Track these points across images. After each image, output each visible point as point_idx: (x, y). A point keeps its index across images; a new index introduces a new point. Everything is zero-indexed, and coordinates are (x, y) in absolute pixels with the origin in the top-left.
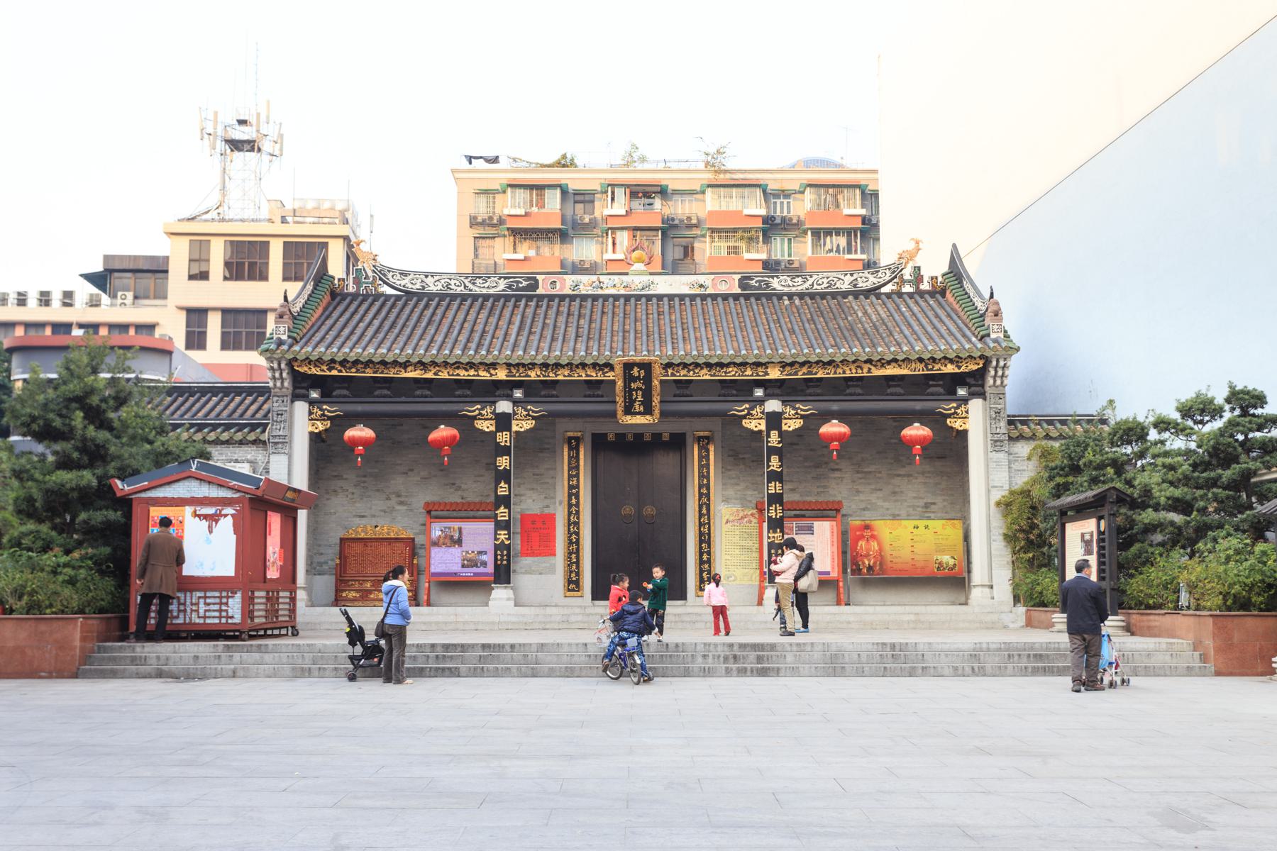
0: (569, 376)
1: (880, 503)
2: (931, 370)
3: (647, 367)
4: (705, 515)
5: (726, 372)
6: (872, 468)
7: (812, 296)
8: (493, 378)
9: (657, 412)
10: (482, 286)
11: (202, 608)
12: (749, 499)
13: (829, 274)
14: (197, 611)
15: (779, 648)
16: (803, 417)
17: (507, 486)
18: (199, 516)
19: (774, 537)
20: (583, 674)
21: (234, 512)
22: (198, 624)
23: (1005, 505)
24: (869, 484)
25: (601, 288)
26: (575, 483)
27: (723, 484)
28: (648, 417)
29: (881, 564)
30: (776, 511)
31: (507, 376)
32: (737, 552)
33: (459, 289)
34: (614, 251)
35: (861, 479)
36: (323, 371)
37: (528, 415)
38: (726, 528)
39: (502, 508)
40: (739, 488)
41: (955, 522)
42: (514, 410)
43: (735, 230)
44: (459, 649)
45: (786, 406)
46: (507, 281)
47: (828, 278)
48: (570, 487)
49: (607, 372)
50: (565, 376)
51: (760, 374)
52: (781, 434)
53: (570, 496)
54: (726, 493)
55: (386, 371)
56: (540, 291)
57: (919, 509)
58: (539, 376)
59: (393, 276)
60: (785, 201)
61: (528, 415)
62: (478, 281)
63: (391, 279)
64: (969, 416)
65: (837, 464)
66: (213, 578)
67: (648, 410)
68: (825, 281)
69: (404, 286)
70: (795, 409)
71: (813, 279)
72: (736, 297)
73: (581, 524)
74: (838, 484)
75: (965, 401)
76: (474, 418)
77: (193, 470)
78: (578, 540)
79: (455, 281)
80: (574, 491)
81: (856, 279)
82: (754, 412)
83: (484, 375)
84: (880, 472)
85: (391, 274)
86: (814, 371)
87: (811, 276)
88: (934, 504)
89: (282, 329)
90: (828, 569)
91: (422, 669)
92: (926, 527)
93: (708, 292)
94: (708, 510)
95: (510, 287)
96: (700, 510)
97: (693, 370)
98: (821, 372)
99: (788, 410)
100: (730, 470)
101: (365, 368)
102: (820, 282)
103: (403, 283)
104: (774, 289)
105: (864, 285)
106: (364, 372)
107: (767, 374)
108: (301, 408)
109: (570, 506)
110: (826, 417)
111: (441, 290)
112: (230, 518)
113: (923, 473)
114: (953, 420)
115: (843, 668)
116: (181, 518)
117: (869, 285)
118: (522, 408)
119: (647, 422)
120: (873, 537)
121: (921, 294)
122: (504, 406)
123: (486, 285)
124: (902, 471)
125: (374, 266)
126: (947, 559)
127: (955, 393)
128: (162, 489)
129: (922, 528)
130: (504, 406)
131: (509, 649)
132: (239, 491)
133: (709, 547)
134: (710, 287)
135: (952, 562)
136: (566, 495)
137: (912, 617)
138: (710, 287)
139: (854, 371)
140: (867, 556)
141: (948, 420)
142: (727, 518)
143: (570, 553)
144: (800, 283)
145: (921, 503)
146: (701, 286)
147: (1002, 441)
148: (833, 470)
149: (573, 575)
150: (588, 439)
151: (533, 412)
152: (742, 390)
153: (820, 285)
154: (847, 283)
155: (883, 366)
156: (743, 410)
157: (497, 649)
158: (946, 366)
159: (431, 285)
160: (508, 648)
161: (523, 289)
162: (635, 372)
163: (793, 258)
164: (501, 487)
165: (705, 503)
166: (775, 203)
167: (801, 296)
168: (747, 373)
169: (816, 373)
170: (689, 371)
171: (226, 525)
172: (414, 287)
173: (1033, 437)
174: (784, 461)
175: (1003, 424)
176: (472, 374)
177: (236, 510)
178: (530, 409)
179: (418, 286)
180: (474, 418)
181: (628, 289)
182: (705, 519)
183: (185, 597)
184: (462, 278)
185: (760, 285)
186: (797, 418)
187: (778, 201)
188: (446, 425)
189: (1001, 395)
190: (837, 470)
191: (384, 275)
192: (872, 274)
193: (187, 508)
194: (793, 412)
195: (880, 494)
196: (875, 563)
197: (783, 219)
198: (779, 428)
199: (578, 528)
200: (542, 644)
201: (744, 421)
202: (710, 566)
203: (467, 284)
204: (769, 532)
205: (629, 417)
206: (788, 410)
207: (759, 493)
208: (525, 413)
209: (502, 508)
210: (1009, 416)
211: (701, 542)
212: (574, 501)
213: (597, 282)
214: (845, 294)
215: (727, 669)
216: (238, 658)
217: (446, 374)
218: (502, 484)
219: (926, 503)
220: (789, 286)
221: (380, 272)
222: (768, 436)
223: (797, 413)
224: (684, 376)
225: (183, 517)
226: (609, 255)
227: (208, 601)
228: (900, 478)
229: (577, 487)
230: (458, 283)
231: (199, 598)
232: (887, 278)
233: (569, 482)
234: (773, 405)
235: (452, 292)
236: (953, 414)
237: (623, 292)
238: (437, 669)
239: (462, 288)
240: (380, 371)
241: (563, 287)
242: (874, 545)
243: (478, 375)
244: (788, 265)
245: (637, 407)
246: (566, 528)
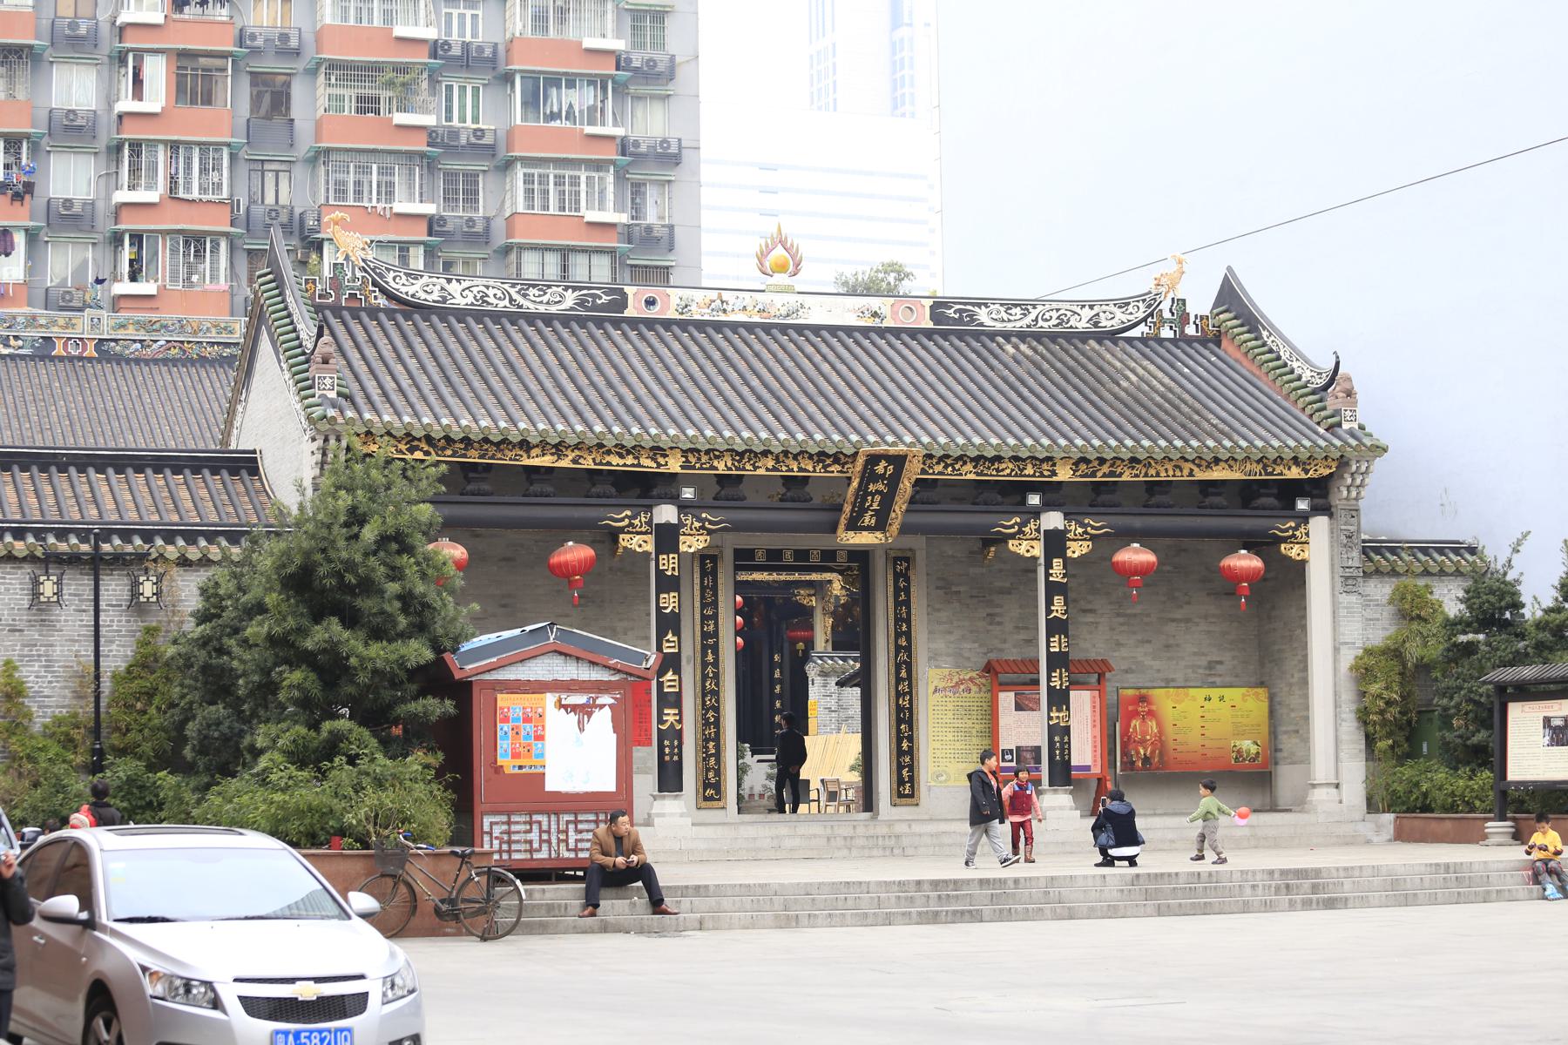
0: (774, 469)
1: (1148, 662)
2: (1271, 474)
3: (899, 461)
4: (904, 680)
5: (997, 470)
6: (1138, 609)
7: (1038, 337)
8: (662, 470)
9: (894, 528)
10: (538, 300)
11: (572, 837)
12: (967, 655)
13: (1060, 305)
14: (566, 841)
15: (1324, 875)
16: (1093, 538)
17: (675, 639)
18: (565, 707)
19: (1058, 717)
20: (1129, 914)
21: (612, 701)
22: (568, 859)
23: (1364, 672)
24: (1134, 633)
25: (725, 311)
26: (711, 628)
27: (930, 632)
28: (879, 534)
29: (1161, 754)
30: (1061, 679)
31: (682, 467)
32: (950, 736)
33: (502, 304)
35: (1122, 624)
36: (401, 452)
37: (703, 527)
38: (935, 699)
39: (671, 673)
40: (952, 638)
41: (1260, 690)
42: (679, 519)
43: (376, 67)
44: (951, 886)
45: (1070, 521)
46: (577, 293)
47: (1058, 310)
48: (705, 636)
49: (829, 465)
50: (767, 470)
51: (1046, 473)
52: (1067, 562)
53: (704, 649)
54: (933, 646)
55: (499, 456)
56: (630, 312)
57: (1201, 671)
58: (730, 469)
59: (394, 279)
60: (469, 13)
61: (703, 527)
62: (532, 291)
63: (392, 284)
64: (1311, 540)
65: (1090, 602)
66: (587, 794)
67: (881, 526)
68: (1055, 314)
69: (413, 296)
70: (1083, 525)
71: (1037, 311)
72: (928, 334)
73: (721, 694)
74: (1091, 633)
75: (1304, 518)
76: (622, 530)
77: (552, 640)
78: (717, 719)
79: (495, 291)
80: (711, 641)
81: (1098, 314)
82: (1027, 530)
83: (648, 464)
84: (1148, 615)
85: (392, 274)
86: (1119, 470)
87: (1034, 307)
88: (1221, 663)
89: (328, 381)
90: (1088, 762)
91: (936, 913)
92: (1221, 699)
93: (885, 324)
94: (909, 672)
95: (581, 303)
96: (898, 672)
97: (952, 465)
98: (1127, 473)
99: (1073, 528)
100: (939, 610)
101: (466, 449)
102: (1047, 316)
103: (411, 290)
104: (981, 324)
105: (1109, 324)
106: (464, 456)
107: (1054, 473)
109: (705, 664)
110: (1125, 536)
111: (472, 304)
112: (607, 711)
113: (1206, 617)
114: (1288, 546)
115: (1415, 895)
116: (540, 710)
117: (1115, 324)
118: (693, 516)
119: (877, 541)
120: (1151, 714)
121: (1189, 341)
122: (666, 513)
123: (545, 299)
124: (1178, 614)
125: (364, 260)
126: (1248, 746)
127: (1293, 506)
128: (513, 668)
129: (1215, 699)
130: (666, 513)
131: (1012, 886)
132: (619, 671)
133: (911, 729)
134: (889, 316)
135: (1254, 749)
136: (699, 647)
137: (1246, 832)
138: (889, 316)
139: (1171, 473)
140: (1143, 742)
141: (1283, 546)
142: (935, 683)
143: (706, 740)
144: (1018, 317)
145: (1203, 661)
146: (875, 315)
147: (1354, 578)
148: (1085, 611)
149: (711, 775)
150: (728, 556)
151: (711, 523)
152: (1015, 492)
153: (1046, 320)
154: (1085, 320)
155: (1208, 466)
156: (1012, 527)
157: (997, 886)
158: (1289, 469)
159: (457, 295)
160: (1011, 884)
161: (603, 308)
162: (880, 469)
163: (481, 126)
164: (668, 641)
165: (905, 662)
166: (449, 15)
167: (1022, 336)
168: (1026, 472)
169: (1120, 475)
170: (946, 467)
171: (602, 720)
172: (429, 298)
173: (1394, 573)
174: (1071, 606)
175: (1355, 554)
176: (629, 463)
177: (615, 699)
178: (706, 519)
179: (435, 296)
180: (622, 530)
181: (765, 314)
182: (903, 687)
183: (549, 821)
184: (506, 286)
185: (961, 317)
186: (1085, 540)
187: (455, 12)
188: (576, 542)
189: (1354, 512)
190: (1091, 611)
191: (381, 276)
192: (1120, 307)
193: (548, 695)
194: (1080, 530)
195: (1148, 648)
196: (1153, 752)
197: (466, 46)
198: (1062, 554)
199: (718, 701)
200: (1052, 878)
201: (1011, 542)
202: (912, 759)
203: (515, 296)
204: (1050, 710)
205: (851, 534)
206: (1073, 528)
207: (980, 646)
208: (697, 525)
209: (671, 673)
210: (1364, 541)
211: (899, 721)
212: (710, 658)
213: (719, 302)
214: (1084, 337)
215: (1290, 900)
216: (688, 905)
217: (590, 459)
218: (670, 636)
219: (1210, 662)
220: (1003, 321)
221: (373, 270)
222: (1049, 565)
223: (1086, 532)
224: (940, 473)
225: (544, 708)
226: (126, 104)
227: (580, 826)
228: (1174, 624)
229: (716, 634)
230: (499, 294)
231: (568, 822)
232: (1141, 315)
233: (702, 628)
234: (1053, 520)
235: (489, 308)
236: (1290, 537)
237: (756, 319)
238: (955, 912)
239: (506, 302)
240: (490, 454)
241: (666, 307)
242: (1152, 725)
243: (639, 465)
244: (473, 140)
245: (867, 519)
246: (699, 701)
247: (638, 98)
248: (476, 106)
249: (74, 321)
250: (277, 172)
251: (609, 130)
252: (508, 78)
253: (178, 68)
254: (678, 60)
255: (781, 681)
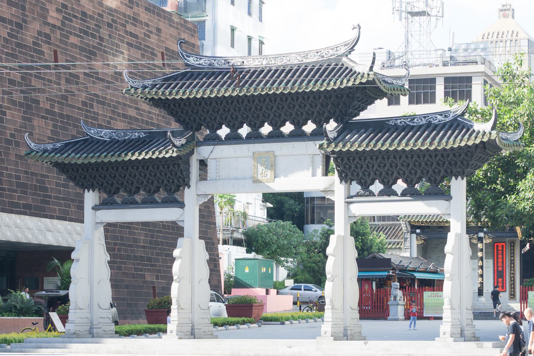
26: (513, 259)
48: (511, 260)
78: (514, 280)
108: (414, 236)
109: (511, 267)
122: (481, 235)
130: (481, 235)
143: (511, 284)
212: (512, 266)
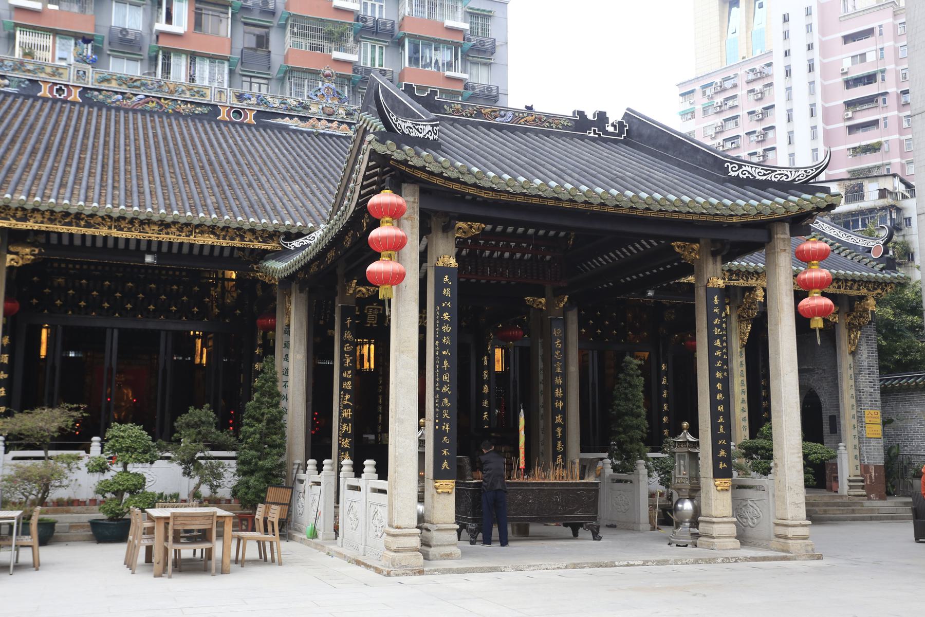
34: (169, 19)
197: (376, 22)
226: (161, 26)
247: (476, 63)
248: (381, 59)
249: (61, 71)
250: (260, 84)
251: (459, 75)
252: (400, 44)
253: (196, 9)
254: (497, 43)
255: (667, 387)
